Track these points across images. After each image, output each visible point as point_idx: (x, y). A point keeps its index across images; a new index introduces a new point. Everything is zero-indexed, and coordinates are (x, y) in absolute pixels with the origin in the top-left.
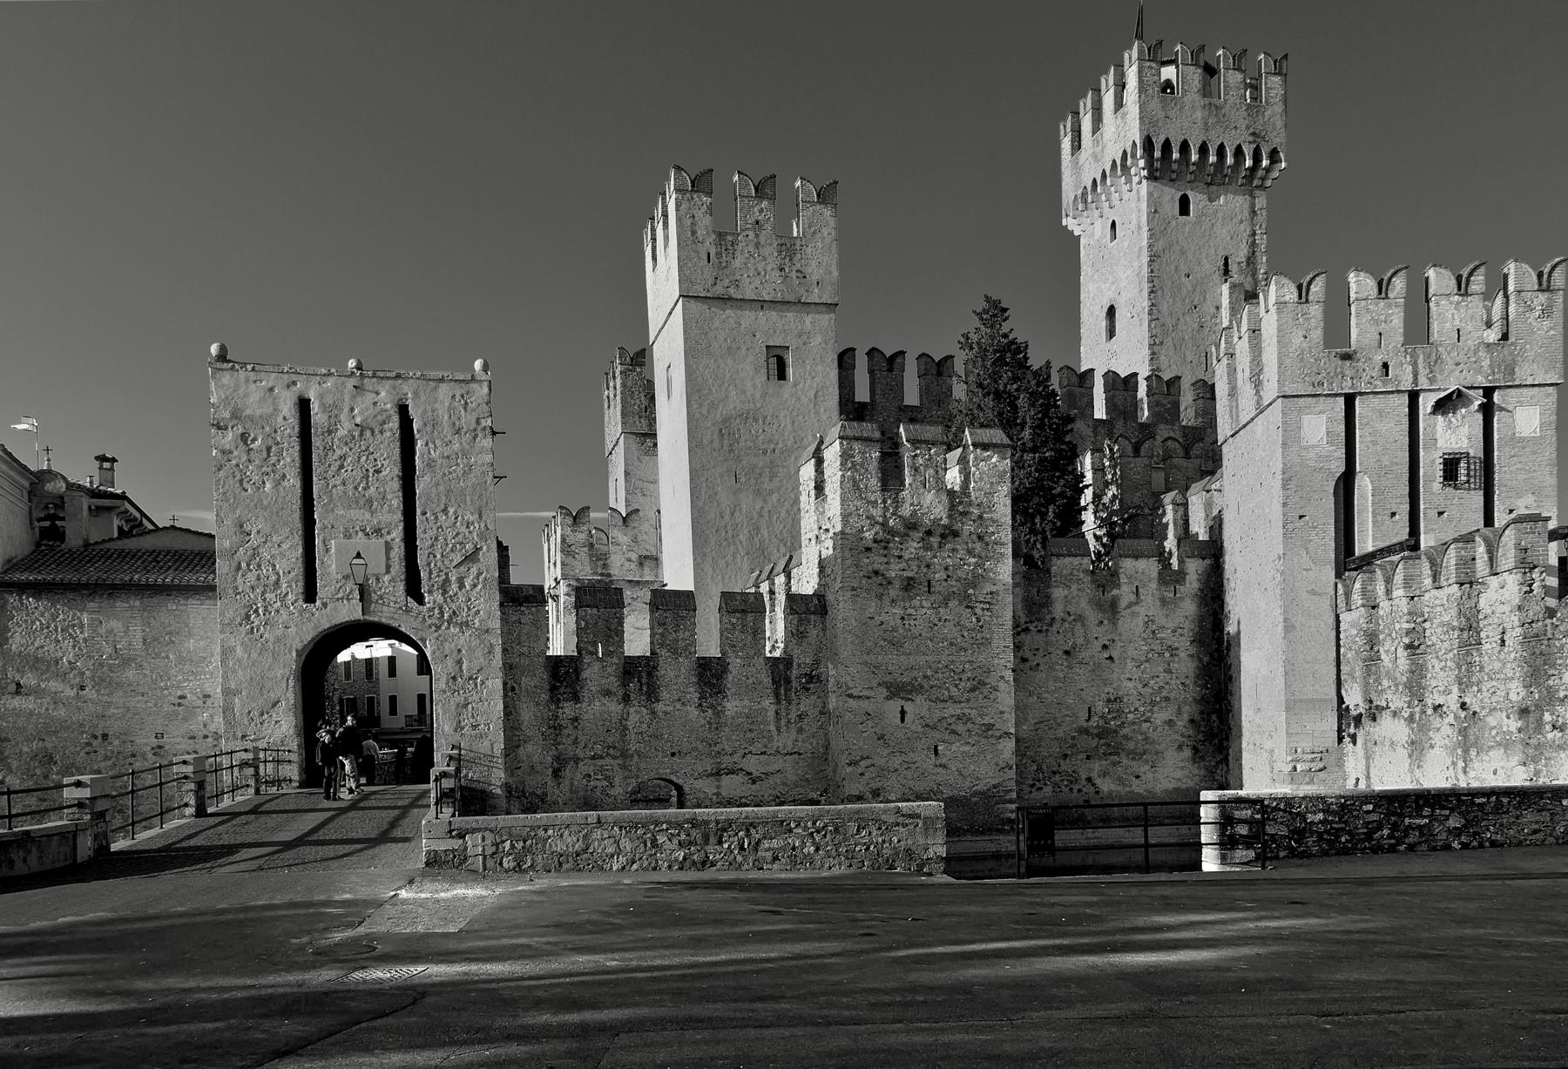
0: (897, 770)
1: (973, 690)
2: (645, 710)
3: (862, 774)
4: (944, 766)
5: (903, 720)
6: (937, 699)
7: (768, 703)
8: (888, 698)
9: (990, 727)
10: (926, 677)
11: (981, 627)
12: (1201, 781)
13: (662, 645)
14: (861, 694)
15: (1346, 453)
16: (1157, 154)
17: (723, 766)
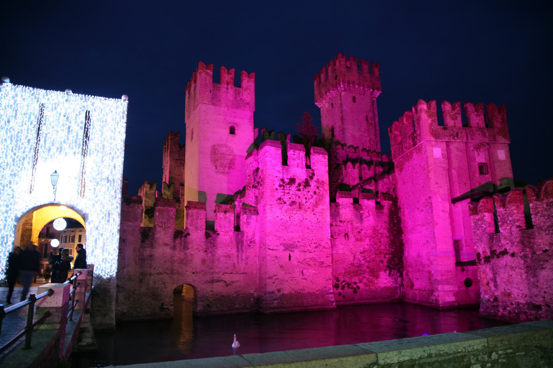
0: (287, 281)
1: (316, 247)
2: (182, 253)
3: (274, 283)
4: (306, 279)
5: (290, 259)
6: (303, 251)
7: (234, 251)
8: (284, 250)
9: (323, 263)
10: (298, 242)
11: (319, 222)
12: (393, 284)
13: (191, 225)
14: (274, 248)
15: (448, 162)
16: (346, 84)
17: (215, 279)
